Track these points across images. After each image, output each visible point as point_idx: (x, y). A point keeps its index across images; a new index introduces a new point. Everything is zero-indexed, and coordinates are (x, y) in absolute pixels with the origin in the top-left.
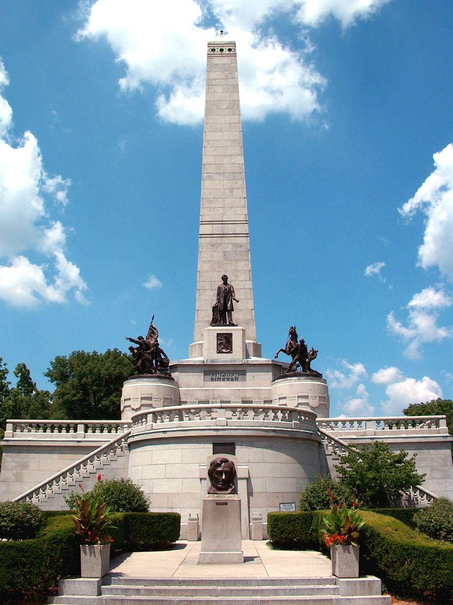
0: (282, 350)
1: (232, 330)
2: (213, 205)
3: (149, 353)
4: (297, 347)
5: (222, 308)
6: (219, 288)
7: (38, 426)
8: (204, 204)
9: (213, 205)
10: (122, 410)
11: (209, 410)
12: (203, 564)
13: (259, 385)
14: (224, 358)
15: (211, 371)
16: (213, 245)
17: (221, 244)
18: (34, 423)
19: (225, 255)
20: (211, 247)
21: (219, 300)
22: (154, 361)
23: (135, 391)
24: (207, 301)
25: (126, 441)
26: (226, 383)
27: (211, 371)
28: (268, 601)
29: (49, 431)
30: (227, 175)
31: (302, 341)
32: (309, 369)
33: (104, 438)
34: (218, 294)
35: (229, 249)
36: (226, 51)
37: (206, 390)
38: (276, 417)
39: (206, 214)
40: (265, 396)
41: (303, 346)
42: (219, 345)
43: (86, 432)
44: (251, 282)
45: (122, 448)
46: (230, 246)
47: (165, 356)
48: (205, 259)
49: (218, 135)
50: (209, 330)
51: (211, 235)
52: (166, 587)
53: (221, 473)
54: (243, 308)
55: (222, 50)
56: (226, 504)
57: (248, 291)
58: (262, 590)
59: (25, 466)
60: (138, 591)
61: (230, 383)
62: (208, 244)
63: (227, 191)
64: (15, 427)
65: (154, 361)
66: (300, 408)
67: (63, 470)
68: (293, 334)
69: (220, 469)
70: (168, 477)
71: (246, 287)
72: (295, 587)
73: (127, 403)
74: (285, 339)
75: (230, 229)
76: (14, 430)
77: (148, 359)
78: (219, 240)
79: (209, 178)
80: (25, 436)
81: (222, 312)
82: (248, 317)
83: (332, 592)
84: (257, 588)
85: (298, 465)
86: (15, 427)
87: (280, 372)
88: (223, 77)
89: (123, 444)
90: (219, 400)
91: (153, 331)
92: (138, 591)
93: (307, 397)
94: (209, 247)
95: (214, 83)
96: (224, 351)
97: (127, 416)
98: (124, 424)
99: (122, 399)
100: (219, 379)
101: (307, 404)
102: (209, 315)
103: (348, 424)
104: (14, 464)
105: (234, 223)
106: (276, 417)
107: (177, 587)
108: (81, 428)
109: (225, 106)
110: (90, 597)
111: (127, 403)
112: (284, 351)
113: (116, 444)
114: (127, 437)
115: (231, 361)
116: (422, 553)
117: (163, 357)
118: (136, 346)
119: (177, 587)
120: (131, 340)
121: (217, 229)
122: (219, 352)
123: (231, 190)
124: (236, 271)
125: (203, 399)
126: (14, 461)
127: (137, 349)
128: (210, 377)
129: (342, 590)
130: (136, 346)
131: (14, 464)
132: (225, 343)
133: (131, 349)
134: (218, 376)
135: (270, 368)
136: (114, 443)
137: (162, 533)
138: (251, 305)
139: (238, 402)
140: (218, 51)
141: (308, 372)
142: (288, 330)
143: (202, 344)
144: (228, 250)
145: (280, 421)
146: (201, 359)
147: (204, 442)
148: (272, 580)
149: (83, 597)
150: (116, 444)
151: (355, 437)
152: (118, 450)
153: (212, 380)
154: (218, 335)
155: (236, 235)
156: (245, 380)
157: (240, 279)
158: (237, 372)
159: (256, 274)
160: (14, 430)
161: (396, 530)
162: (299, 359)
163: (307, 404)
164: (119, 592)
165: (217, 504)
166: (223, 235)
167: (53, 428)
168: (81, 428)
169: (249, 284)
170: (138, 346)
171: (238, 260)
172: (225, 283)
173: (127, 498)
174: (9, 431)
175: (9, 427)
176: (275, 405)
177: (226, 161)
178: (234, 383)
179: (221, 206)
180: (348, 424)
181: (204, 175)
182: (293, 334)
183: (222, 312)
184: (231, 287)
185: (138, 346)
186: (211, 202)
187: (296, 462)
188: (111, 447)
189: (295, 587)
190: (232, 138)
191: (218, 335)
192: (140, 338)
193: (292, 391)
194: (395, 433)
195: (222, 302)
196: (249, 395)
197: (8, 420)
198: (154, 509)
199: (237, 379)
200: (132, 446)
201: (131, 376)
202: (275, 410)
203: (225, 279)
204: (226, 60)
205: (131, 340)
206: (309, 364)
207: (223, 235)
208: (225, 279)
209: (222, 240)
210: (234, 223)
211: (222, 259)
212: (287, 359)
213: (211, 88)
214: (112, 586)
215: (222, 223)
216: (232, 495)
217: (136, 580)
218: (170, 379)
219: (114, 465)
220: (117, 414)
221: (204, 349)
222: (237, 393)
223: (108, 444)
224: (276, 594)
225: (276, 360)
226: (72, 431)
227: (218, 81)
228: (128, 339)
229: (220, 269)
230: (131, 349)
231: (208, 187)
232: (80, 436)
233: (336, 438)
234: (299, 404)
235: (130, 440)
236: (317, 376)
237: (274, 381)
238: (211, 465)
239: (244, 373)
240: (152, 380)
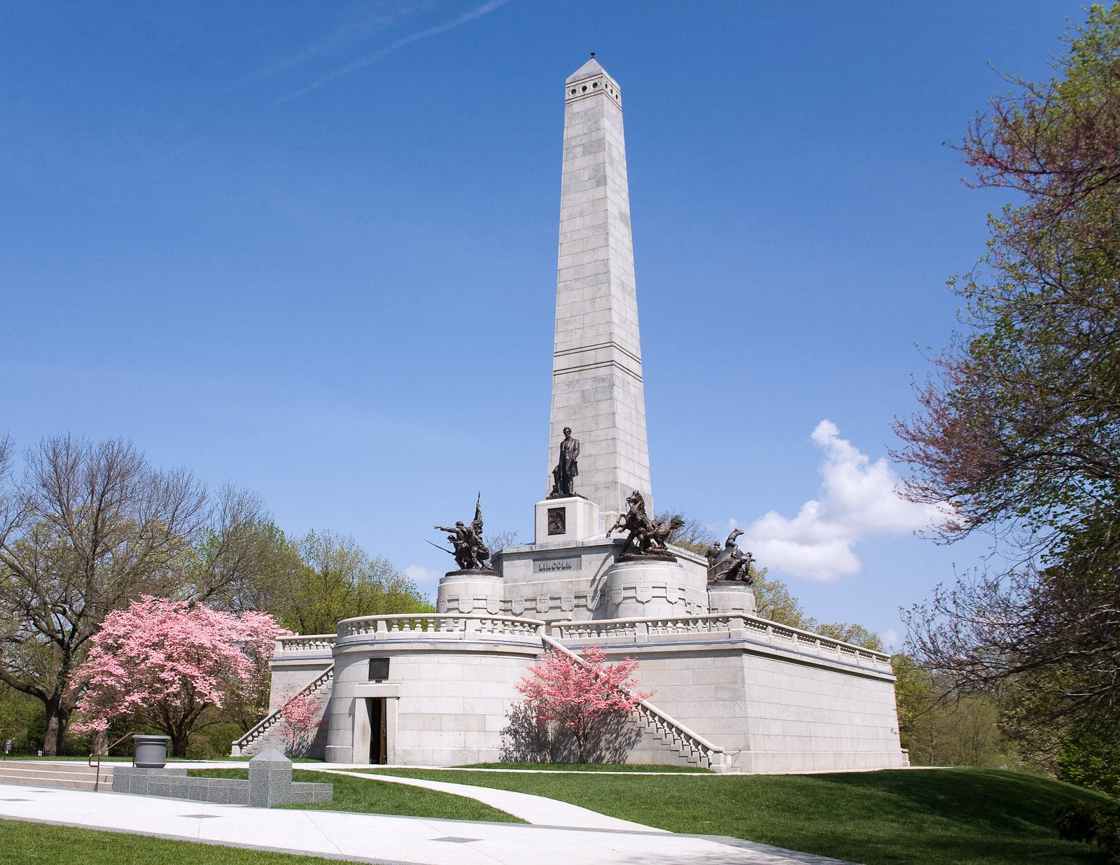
2: (569, 327)
8: (560, 326)
9: (569, 327)
14: (557, 542)
17: (578, 381)
19: (583, 397)
20: (567, 387)
36: (590, 89)
37: (534, 584)
49: (578, 222)
51: (567, 370)
55: (584, 89)
62: (563, 383)
63: (588, 303)
71: (608, 437)
75: (590, 357)
78: (576, 376)
79: (566, 287)
88: (585, 131)
90: (548, 597)
95: (573, 143)
115: (564, 544)
122: (551, 533)
124: (597, 416)
125: (531, 597)
135: (611, 549)
140: (580, 92)
144: (587, 388)
157: (601, 426)
171: (599, 401)
179: (579, 326)
181: (560, 285)
186: (567, 323)
203: (567, 432)
204: (589, 103)
207: (581, 368)
208: (567, 432)
209: (580, 375)
211: (580, 401)
213: (570, 153)
215: (581, 350)
222: (570, 586)
227: (579, 139)
229: (576, 417)
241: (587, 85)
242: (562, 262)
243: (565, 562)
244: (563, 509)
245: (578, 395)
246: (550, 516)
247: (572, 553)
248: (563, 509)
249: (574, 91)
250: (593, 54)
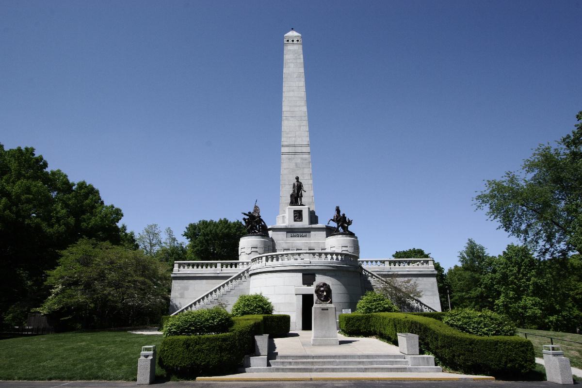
0: (331, 220)
1: (302, 208)
3: (255, 222)
4: (341, 218)
5: (296, 196)
6: (294, 184)
7: (189, 265)
8: (284, 135)
10: (239, 254)
11: (299, 254)
12: (315, 345)
13: (318, 240)
14: (298, 225)
15: (290, 231)
16: (289, 159)
17: (294, 158)
18: (205, 263)
19: (296, 165)
21: (294, 191)
22: (258, 226)
23: (247, 243)
24: (287, 191)
25: (248, 272)
26: (299, 238)
27: (290, 231)
28: (369, 368)
29: (195, 267)
30: (297, 118)
31: (344, 215)
32: (348, 231)
33: (233, 271)
34: (294, 187)
35: (299, 161)
38: (332, 258)
39: (285, 141)
40: (322, 246)
41: (344, 217)
42: (295, 217)
43: (222, 267)
44: (312, 181)
45: (245, 277)
46: (300, 160)
47: (264, 222)
48: (285, 167)
49: (291, 94)
50: (289, 208)
51: (288, 153)
52: (305, 360)
53: (323, 291)
54: (307, 197)
55: (293, 41)
56: (327, 309)
57: (310, 186)
58: (363, 362)
59: (186, 289)
60: (290, 363)
61: (302, 238)
64: (180, 265)
65: (258, 226)
66: (343, 252)
67: (211, 291)
68: (338, 210)
69: (322, 289)
70: (282, 293)
72: (381, 360)
73: (243, 250)
74: (334, 214)
75: (299, 150)
76: (179, 267)
77: (254, 224)
79: (287, 119)
80: (185, 271)
81: (296, 198)
82: (311, 200)
83: (404, 364)
84: (358, 360)
85: (343, 287)
86: (180, 265)
87: (330, 232)
89: (246, 274)
90: (295, 249)
91: (256, 209)
92: (290, 363)
93: (347, 247)
94: (287, 160)
96: (298, 220)
97: (243, 258)
98: (239, 263)
99: (240, 248)
100: (295, 236)
101: (347, 251)
102: (289, 200)
103: (374, 263)
104: (179, 288)
105: (301, 146)
106: (332, 258)
107: (312, 360)
108: (219, 265)
109: (295, 76)
110: (263, 367)
111: (243, 250)
112: (333, 220)
113: (242, 275)
114: (247, 270)
116: (461, 341)
117: (263, 223)
118: (247, 217)
119: (312, 360)
120: (245, 214)
121: (291, 150)
122: (295, 221)
123: (300, 126)
126: (179, 286)
127: (248, 219)
128: (289, 234)
129: (410, 363)
130: (247, 217)
131: (179, 288)
132: (298, 215)
133: (244, 219)
134: (295, 234)
136: (240, 274)
137: (279, 327)
138: (312, 193)
139: (306, 250)
140: (290, 41)
141: (347, 232)
142: (335, 209)
143: (284, 216)
145: (335, 260)
146: (284, 225)
147: (299, 272)
148: (368, 356)
149: (259, 367)
150: (242, 275)
151: (379, 270)
152: (243, 278)
153: (292, 237)
154: (294, 211)
155: (302, 153)
156: (310, 237)
157: (305, 179)
158: (305, 231)
159: (314, 175)
160: (179, 267)
161: (440, 326)
162: (341, 225)
163: (347, 251)
164: (279, 364)
165: (323, 309)
166: (295, 153)
167: (207, 265)
168: (219, 265)
169: (311, 182)
170: (248, 217)
172: (298, 181)
173: (260, 305)
174: (176, 268)
175: (176, 266)
176: (327, 251)
177: (297, 109)
178: (304, 238)
180: (374, 263)
181: (284, 118)
182: (338, 210)
183: (296, 198)
184: (301, 183)
185: (248, 217)
186: (288, 134)
187: (341, 284)
188: (239, 277)
189: (381, 360)
190: (299, 95)
191: (294, 211)
192: (250, 213)
193: (337, 244)
194: (402, 268)
195: (296, 192)
196: (312, 246)
197: (175, 262)
198: (275, 313)
199: (306, 236)
200: (251, 275)
201: (244, 235)
202: (326, 254)
203: (297, 178)
205: (245, 214)
206: (347, 227)
207: (295, 153)
208: (297, 178)
210: (301, 146)
212: (334, 225)
214: (277, 360)
215: (295, 146)
216: (331, 304)
217: (288, 356)
218: (267, 235)
219: (241, 287)
220: (236, 256)
221: (284, 217)
222: (306, 244)
223: (237, 274)
224: (372, 364)
225: (329, 225)
226: (214, 267)
227: (291, 60)
228: (243, 213)
230: (244, 219)
231: (286, 125)
232: (218, 269)
233: (369, 271)
234: (342, 251)
235: (250, 273)
236: (351, 234)
237: (327, 237)
238: (317, 286)
239: (310, 232)
240: (257, 237)
241: (294, 39)
242: (284, 109)
243: (304, 234)
244: (302, 211)
245: (294, 164)
246: (294, 214)
247: (307, 230)
248: (302, 211)
249: (288, 41)
250: (292, 29)
